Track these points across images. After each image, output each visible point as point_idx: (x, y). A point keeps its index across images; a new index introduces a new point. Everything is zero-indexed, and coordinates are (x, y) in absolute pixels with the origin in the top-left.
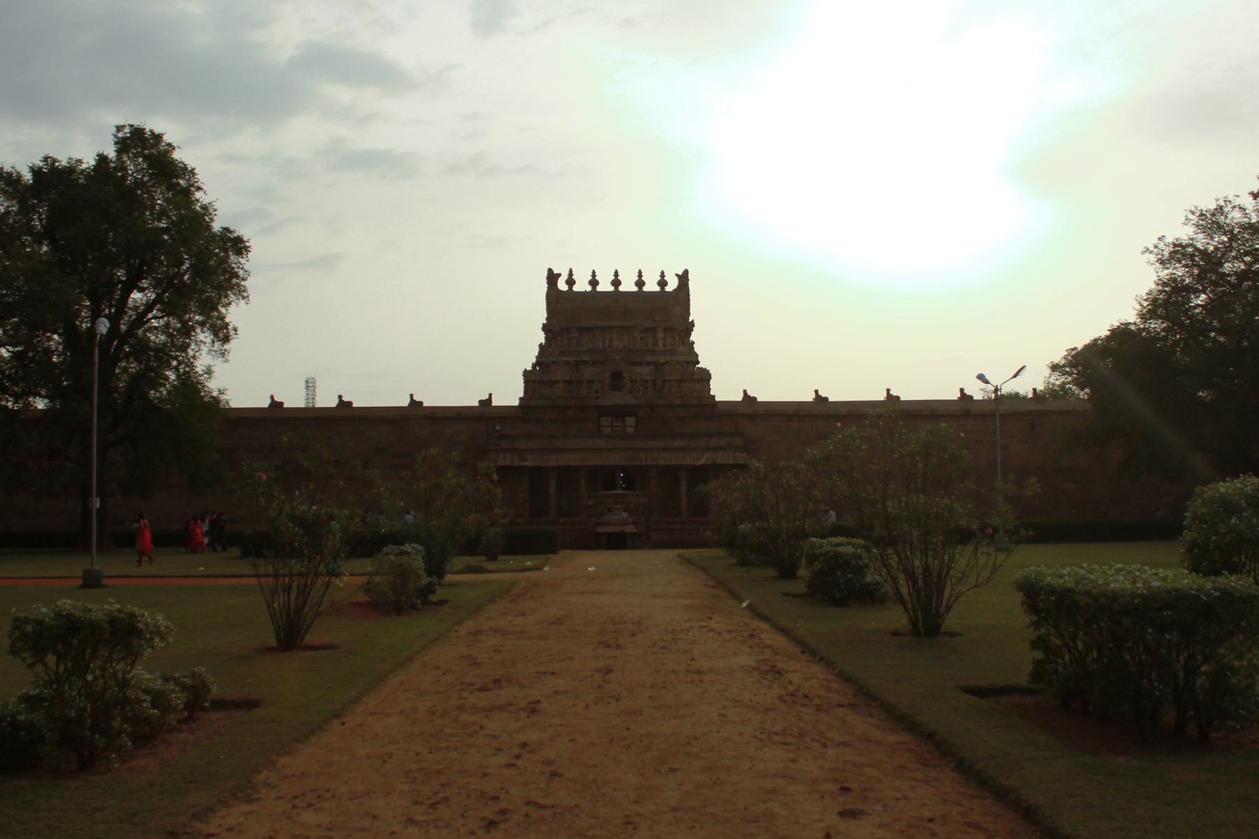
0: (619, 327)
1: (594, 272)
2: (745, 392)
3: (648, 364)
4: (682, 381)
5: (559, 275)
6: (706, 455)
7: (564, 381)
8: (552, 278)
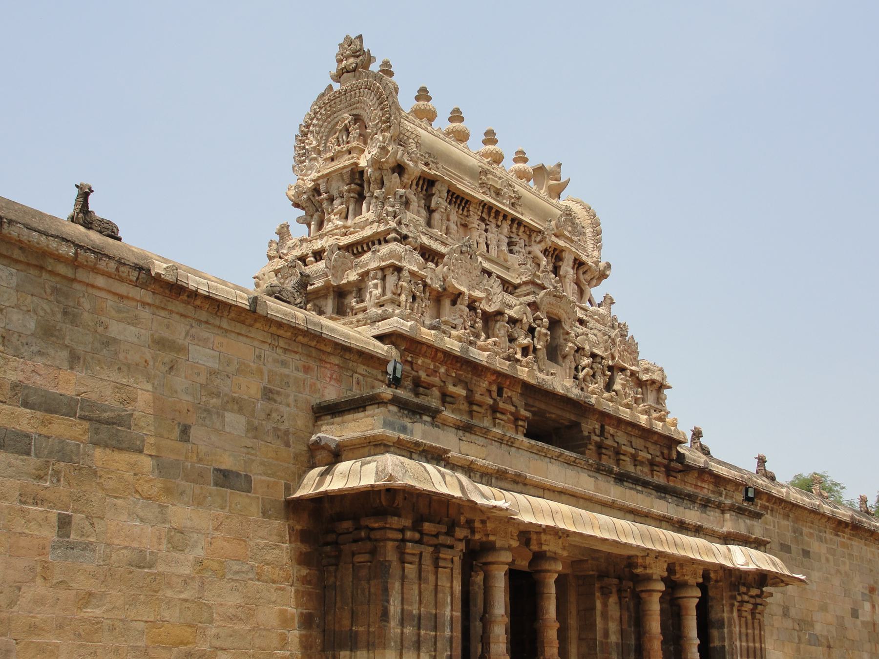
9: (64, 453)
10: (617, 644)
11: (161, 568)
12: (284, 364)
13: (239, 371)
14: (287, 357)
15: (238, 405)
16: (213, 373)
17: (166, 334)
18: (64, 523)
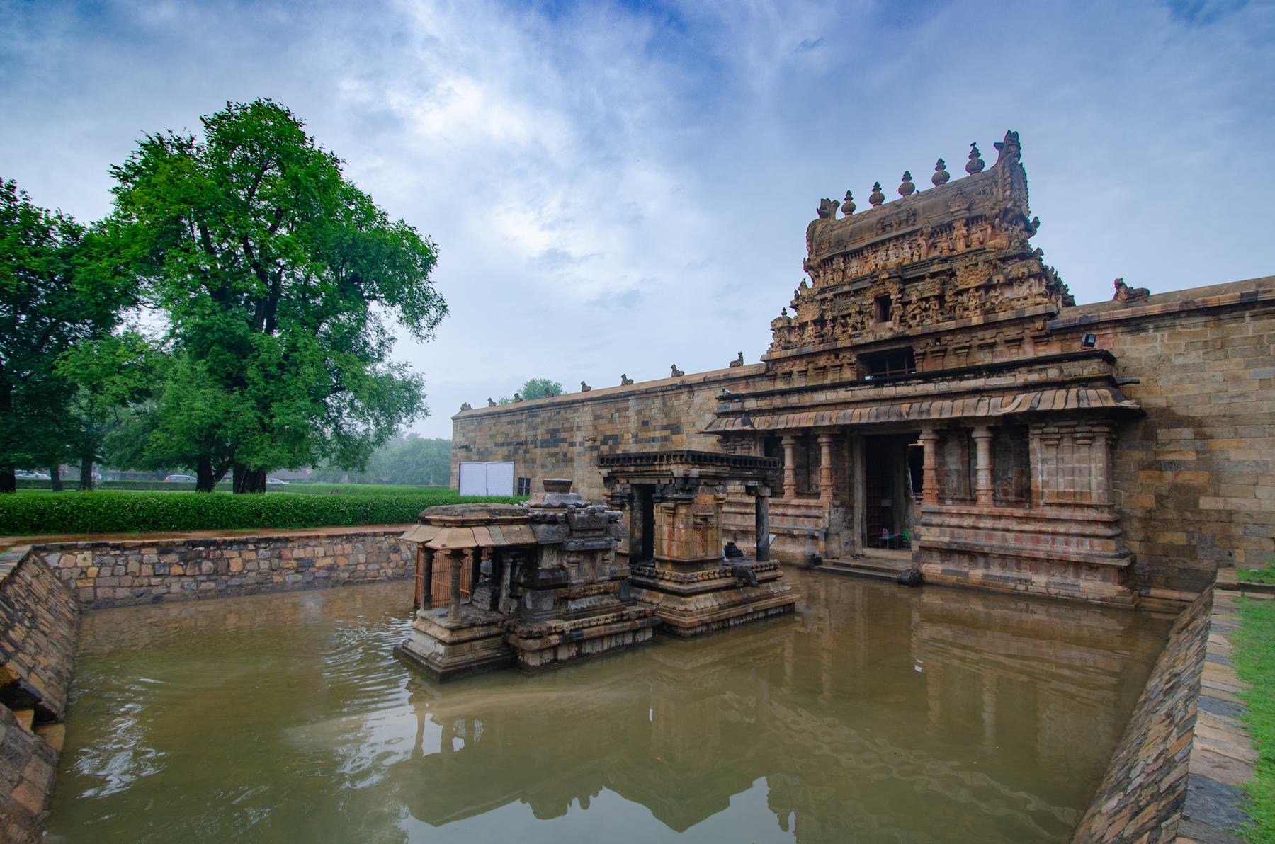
0: (897, 238)
1: (877, 185)
2: (1119, 284)
3: (933, 275)
4: (988, 287)
5: (837, 204)
6: (1020, 398)
7: (814, 322)
8: (826, 209)
10: (958, 471)
15: (709, 410)
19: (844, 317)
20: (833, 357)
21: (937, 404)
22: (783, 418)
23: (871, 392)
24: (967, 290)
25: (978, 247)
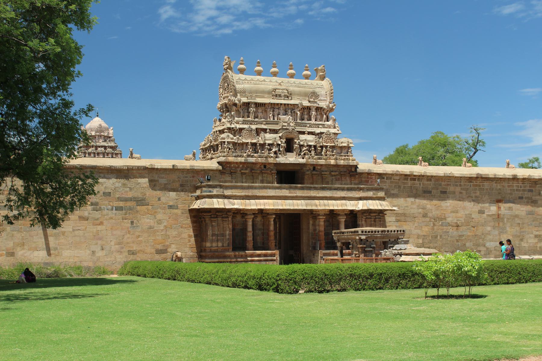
0: (285, 104)
3: (309, 133)
9: (130, 209)
11: (155, 228)
12: (186, 177)
13: (173, 182)
14: (187, 175)
16: (165, 184)
17: (153, 178)
18: (132, 223)
19: (269, 145)
20: (262, 166)
21: (330, 202)
22: (253, 201)
23: (299, 193)
24: (326, 147)
25: (321, 123)
